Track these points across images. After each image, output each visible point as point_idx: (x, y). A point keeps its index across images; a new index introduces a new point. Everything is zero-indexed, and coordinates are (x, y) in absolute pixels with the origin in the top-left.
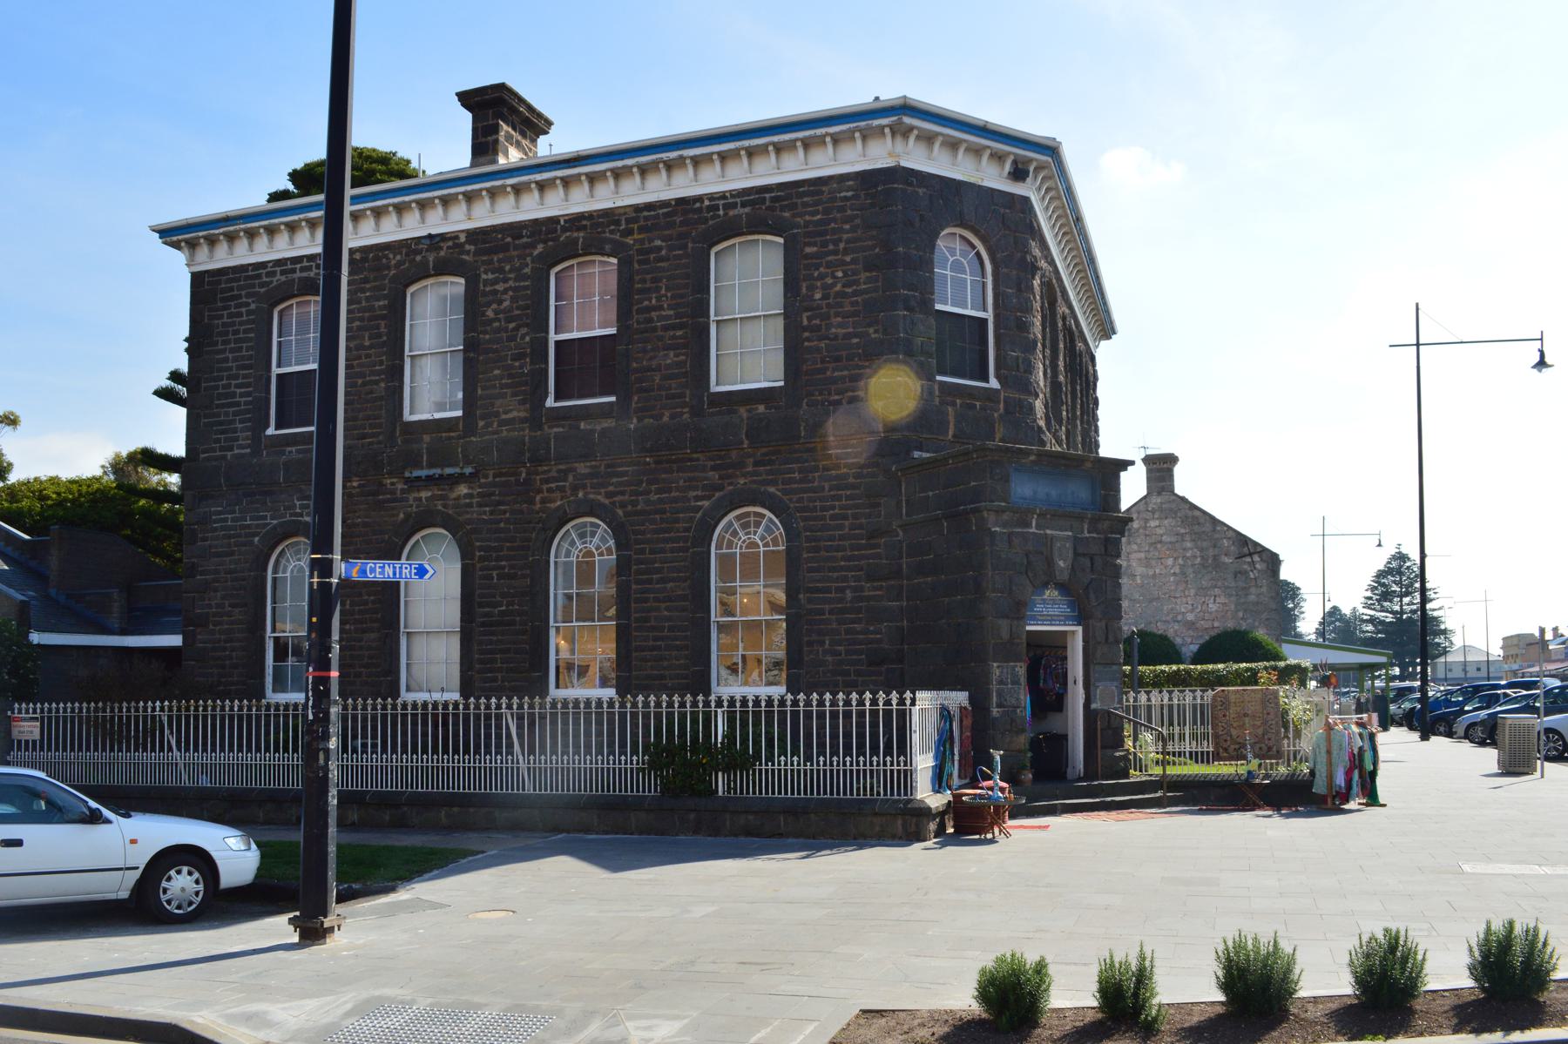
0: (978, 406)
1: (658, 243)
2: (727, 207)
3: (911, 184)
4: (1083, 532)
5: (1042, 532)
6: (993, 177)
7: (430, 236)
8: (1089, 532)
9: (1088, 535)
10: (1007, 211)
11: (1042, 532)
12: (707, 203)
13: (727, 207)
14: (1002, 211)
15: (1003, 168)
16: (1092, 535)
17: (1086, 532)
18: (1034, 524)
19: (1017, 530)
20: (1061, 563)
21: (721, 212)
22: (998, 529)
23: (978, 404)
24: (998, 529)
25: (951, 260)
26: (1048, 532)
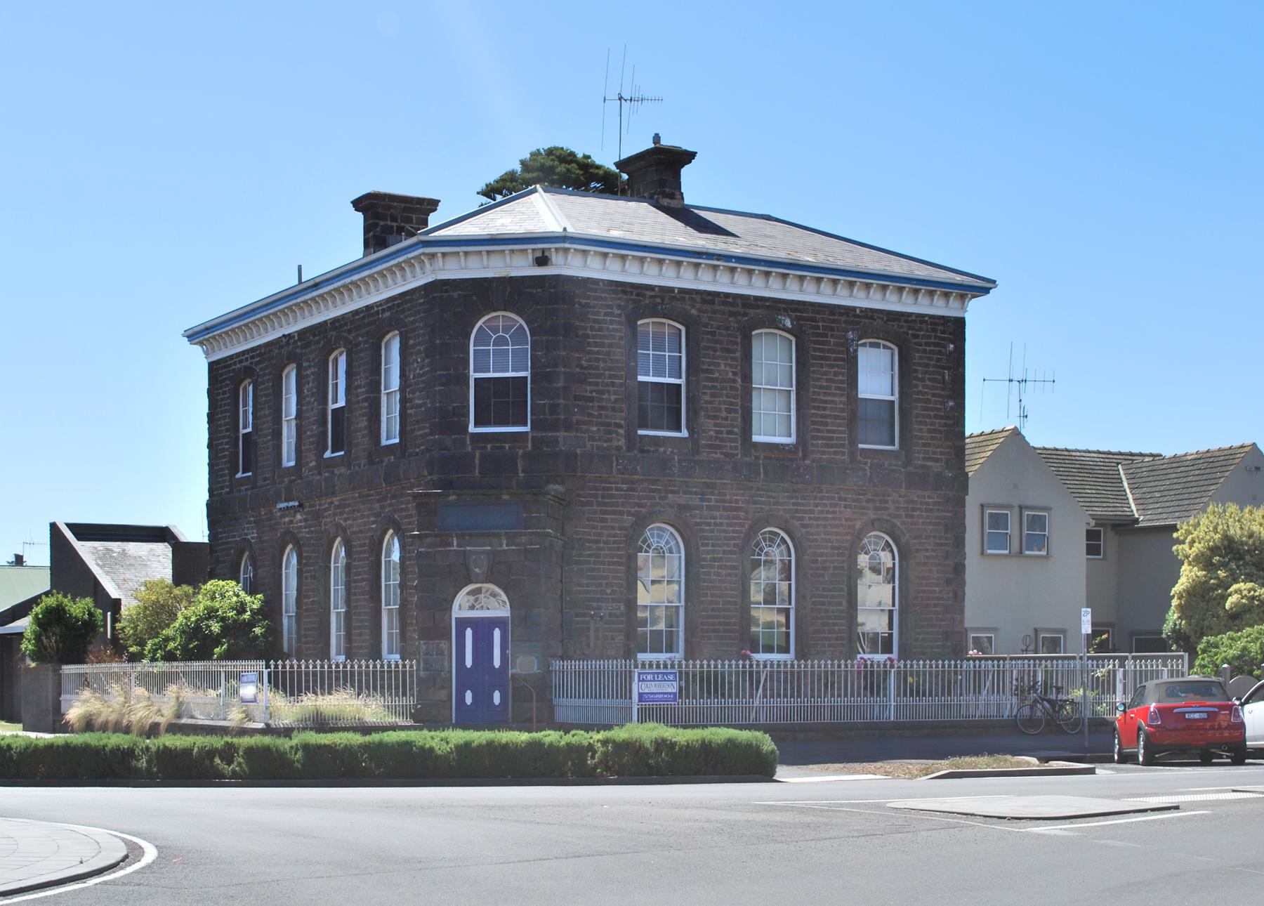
0: (507, 448)
1: (360, 339)
2: (383, 311)
3: (446, 291)
4: (501, 546)
5: (463, 549)
6: (522, 267)
7: (284, 336)
8: (507, 546)
9: (506, 548)
10: (539, 290)
11: (463, 549)
12: (376, 309)
13: (383, 311)
14: (534, 291)
15: (528, 258)
16: (511, 548)
17: (504, 546)
18: (455, 544)
19: (440, 549)
20: (477, 570)
21: (380, 316)
22: (423, 550)
23: (507, 446)
24: (423, 550)
25: (494, 337)
26: (468, 548)
